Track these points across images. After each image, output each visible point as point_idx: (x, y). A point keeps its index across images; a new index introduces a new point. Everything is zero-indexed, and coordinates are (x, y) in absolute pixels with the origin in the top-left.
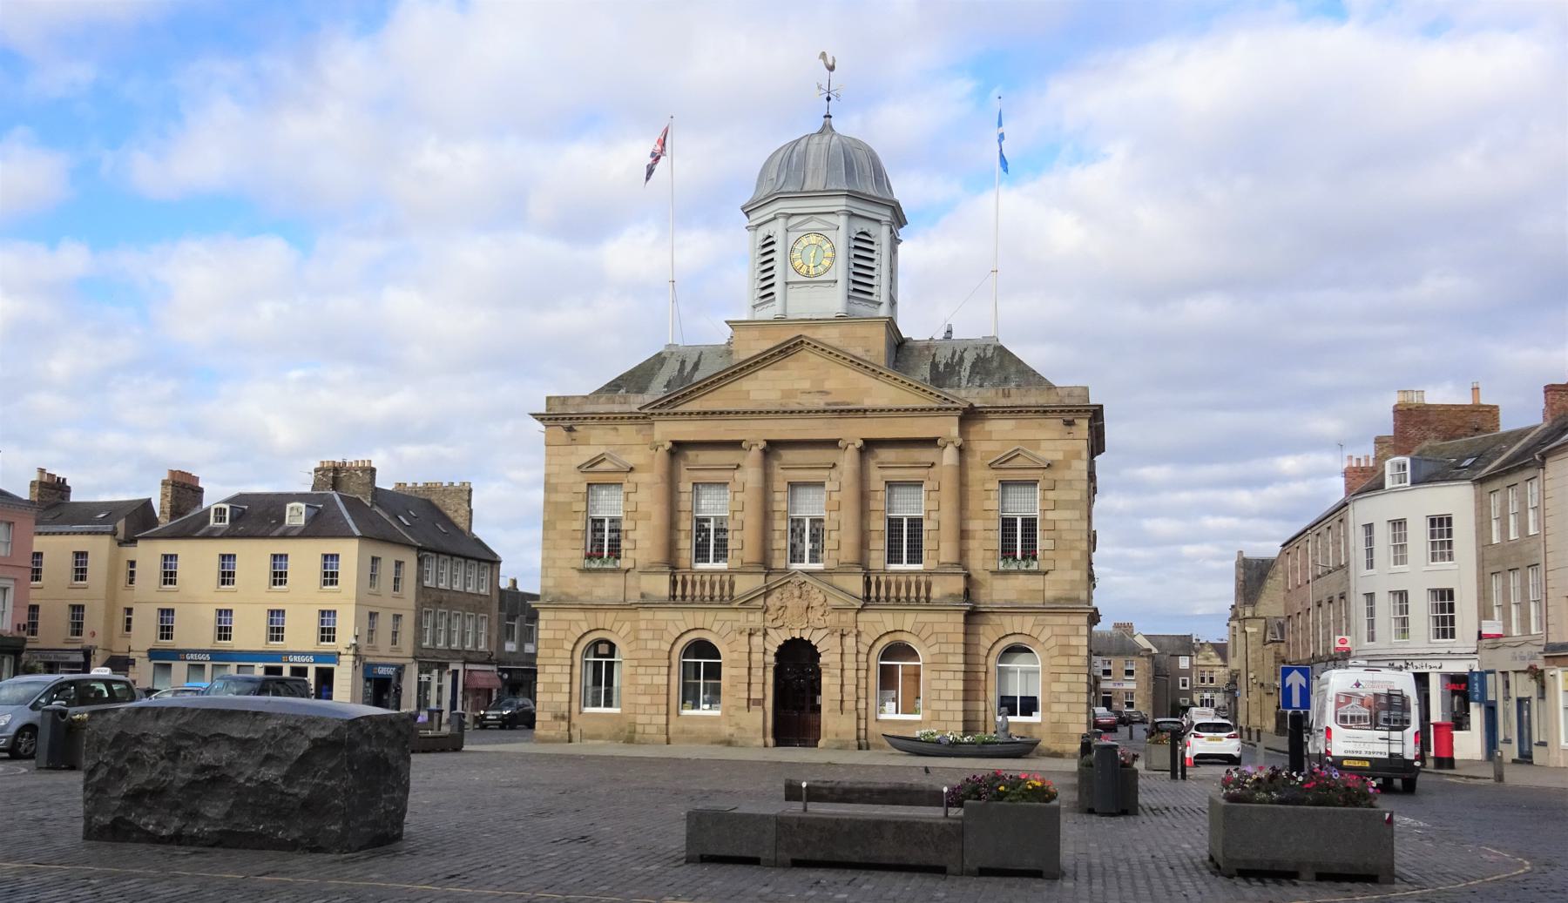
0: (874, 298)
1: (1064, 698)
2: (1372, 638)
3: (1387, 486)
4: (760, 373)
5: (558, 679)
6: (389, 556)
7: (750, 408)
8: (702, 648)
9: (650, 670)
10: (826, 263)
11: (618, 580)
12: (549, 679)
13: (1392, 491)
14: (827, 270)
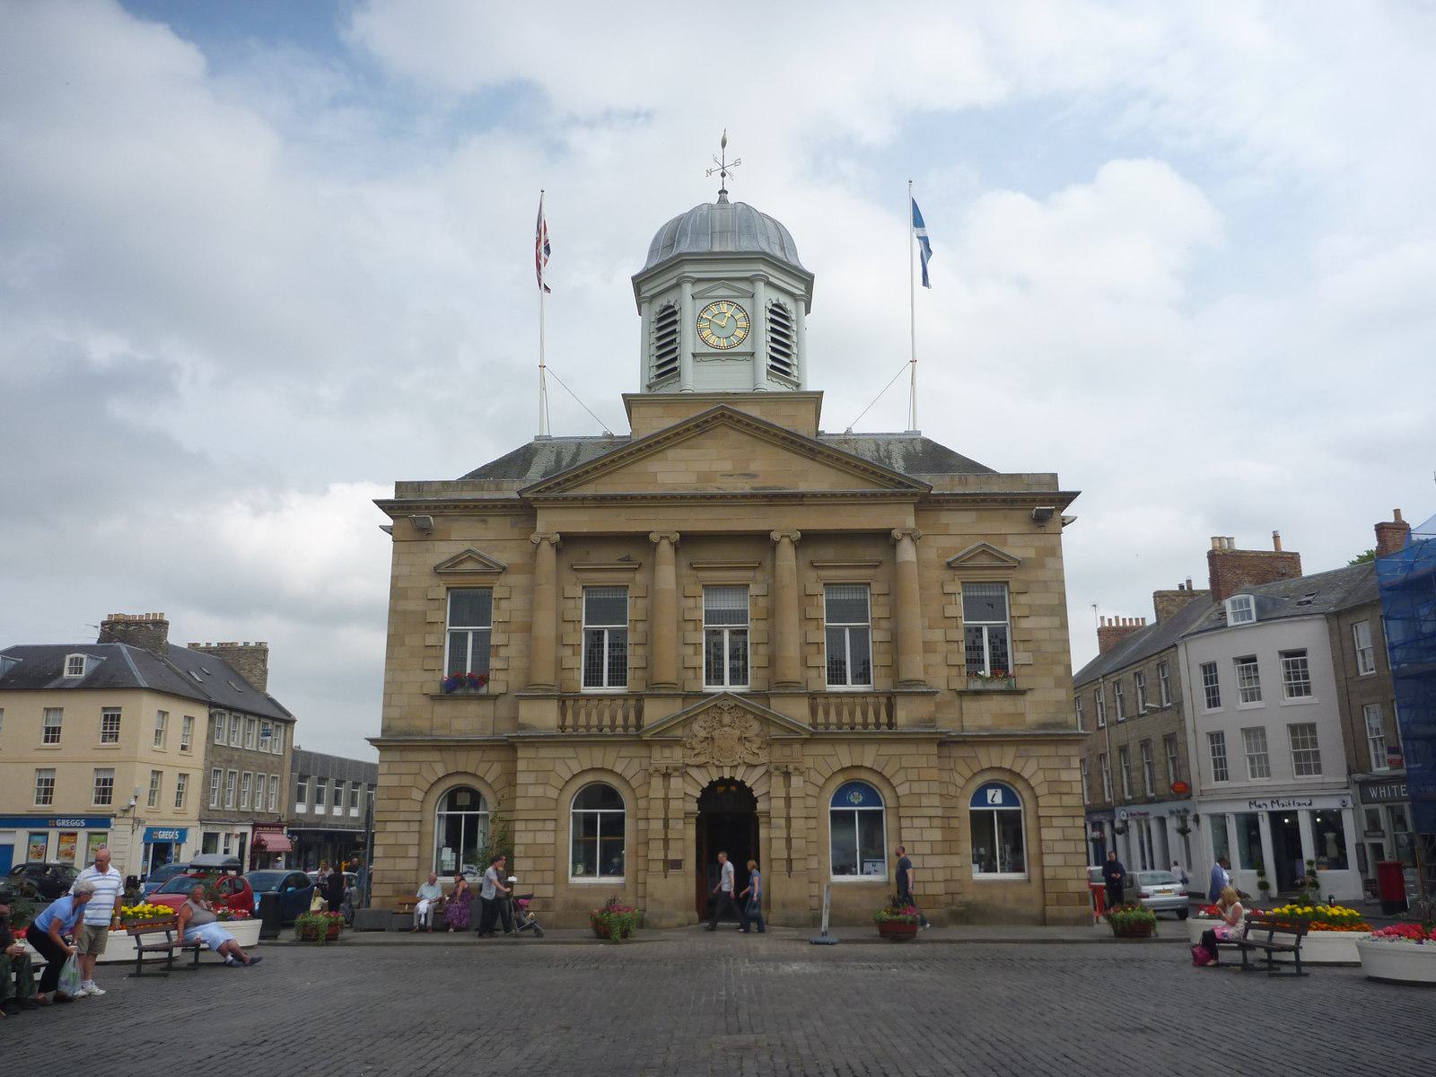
0: (795, 379)
1: (1059, 847)
2: (1222, 775)
3: (1231, 622)
4: (671, 453)
5: (403, 839)
6: (178, 710)
7: (660, 491)
8: (600, 794)
9: (531, 826)
10: (740, 333)
11: (486, 709)
12: (391, 840)
13: (1235, 628)
14: (741, 341)
